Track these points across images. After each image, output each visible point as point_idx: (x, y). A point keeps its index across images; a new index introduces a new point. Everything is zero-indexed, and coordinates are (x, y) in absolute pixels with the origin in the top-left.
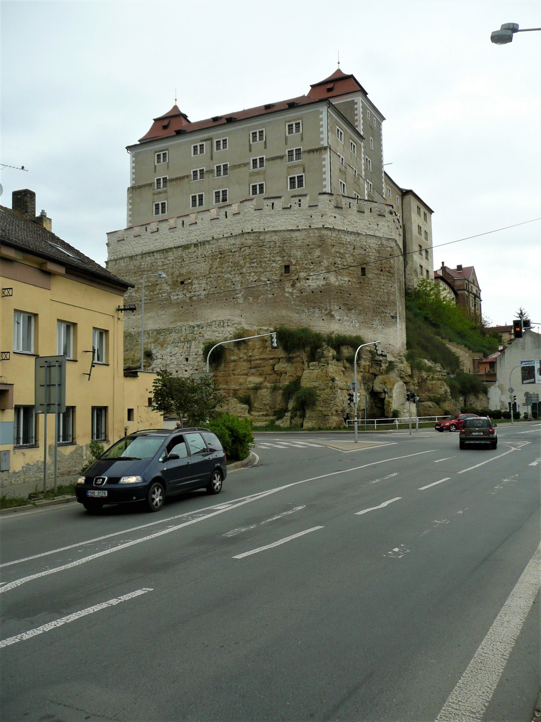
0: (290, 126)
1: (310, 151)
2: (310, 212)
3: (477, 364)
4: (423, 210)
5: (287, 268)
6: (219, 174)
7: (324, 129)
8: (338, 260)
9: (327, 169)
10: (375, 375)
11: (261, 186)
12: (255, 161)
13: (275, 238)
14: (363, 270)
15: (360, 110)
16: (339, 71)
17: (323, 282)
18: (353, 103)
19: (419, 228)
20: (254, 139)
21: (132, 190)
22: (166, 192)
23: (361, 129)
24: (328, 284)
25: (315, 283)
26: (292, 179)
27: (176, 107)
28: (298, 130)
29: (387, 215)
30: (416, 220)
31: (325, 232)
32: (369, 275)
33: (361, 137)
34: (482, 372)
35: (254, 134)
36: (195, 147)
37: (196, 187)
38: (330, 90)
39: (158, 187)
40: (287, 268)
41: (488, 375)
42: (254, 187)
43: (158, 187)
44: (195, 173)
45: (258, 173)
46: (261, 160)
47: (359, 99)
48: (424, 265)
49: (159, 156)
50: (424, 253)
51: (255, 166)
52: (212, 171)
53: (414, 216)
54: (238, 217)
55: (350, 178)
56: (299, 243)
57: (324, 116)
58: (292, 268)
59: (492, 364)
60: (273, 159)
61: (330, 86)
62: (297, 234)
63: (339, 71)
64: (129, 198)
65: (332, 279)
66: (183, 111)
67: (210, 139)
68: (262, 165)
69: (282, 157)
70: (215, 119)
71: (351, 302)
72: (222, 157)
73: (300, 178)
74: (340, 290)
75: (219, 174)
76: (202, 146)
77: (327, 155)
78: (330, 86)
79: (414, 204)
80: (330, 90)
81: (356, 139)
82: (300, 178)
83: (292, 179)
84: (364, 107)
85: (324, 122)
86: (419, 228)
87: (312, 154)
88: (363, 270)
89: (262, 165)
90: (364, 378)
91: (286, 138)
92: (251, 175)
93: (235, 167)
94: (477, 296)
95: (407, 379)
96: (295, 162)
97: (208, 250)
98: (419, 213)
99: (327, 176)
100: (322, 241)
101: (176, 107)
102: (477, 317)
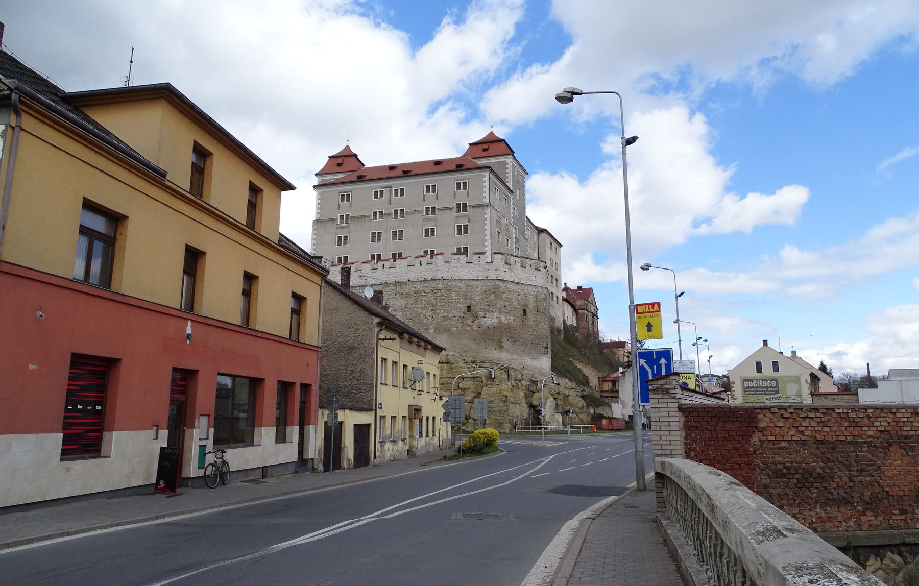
0: (459, 184)
1: (474, 206)
2: (487, 266)
3: (602, 381)
4: (554, 244)
5: (469, 308)
6: (396, 217)
7: (486, 190)
8: (507, 304)
9: (488, 222)
10: (533, 392)
11: (433, 230)
12: (427, 209)
13: (459, 284)
14: (525, 311)
15: (509, 166)
16: (492, 134)
17: (496, 321)
18: (505, 163)
19: (552, 260)
20: (428, 191)
21: (317, 222)
22: (348, 227)
23: (510, 185)
24: (500, 322)
25: (491, 320)
26: (459, 227)
27: (348, 147)
28: (465, 188)
29: (542, 269)
30: (549, 254)
31: (498, 283)
32: (529, 315)
33: (511, 192)
34: (606, 389)
35: (428, 187)
36: (376, 192)
37: (376, 226)
38: (485, 150)
39: (341, 222)
40: (469, 308)
41: (612, 391)
42: (427, 230)
43: (341, 222)
44: (375, 213)
45: (430, 219)
46: (433, 208)
47: (509, 160)
48: (555, 292)
49: (342, 196)
50: (554, 282)
51: (427, 213)
52: (390, 214)
53: (548, 251)
54: (430, 266)
55: (503, 228)
56: (479, 289)
57: (486, 179)
58: (472, 308)
59: (614, 382)
60: (444, 209)
61: (485, 146)
62: (477, 282)
63: (492, 134)
64: (314, 229)
65: (503, 319)
66: (354, 150)
67: (390, 187)
68: (433, 213)
69: (451, 209)
70: (392, 168)
71: (516, 336)
72: (398, 203)
73: (466, 226)
74: (509, 327)
75: (396, 217)
76: (382, 192)
77: (488, 211)
78: (485, 146)
79: (548, 239)
80: (485, 150)
81: (508, 193)
82: (466, 226)
83: (459, 227)
84: (513, 167)
85: (486, 184)
86: (552, 260)
87: (476, 209)
88: (525, 311)
89: (433, 213)
90: (525, 394)
91: (455, 193)
92: (424, 220)
93: (410, 213)
94: (595, 315)
95: (556, 396)
96: (462, 213)
97: (404, 290)
98: (551, 249)
99: (488, 227)
100: (495, 289)
101: (348, 147)
102: (596, 333)
